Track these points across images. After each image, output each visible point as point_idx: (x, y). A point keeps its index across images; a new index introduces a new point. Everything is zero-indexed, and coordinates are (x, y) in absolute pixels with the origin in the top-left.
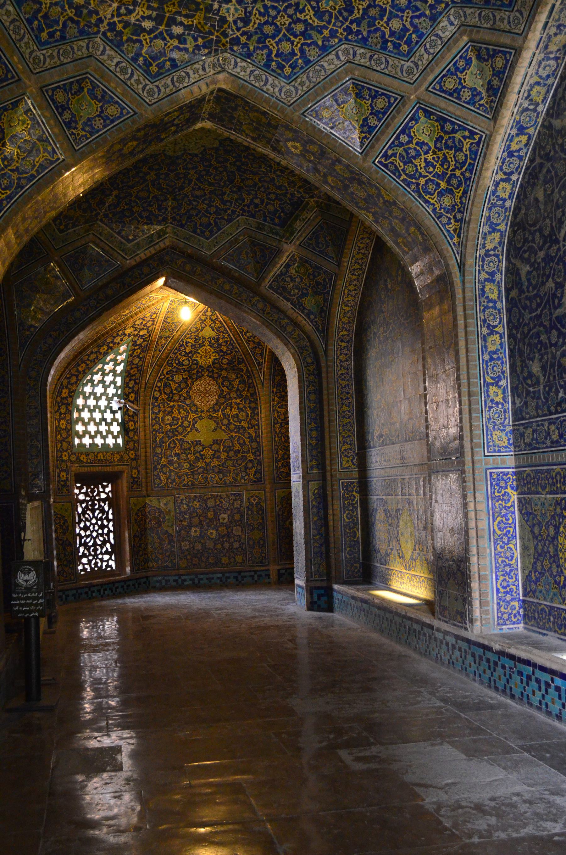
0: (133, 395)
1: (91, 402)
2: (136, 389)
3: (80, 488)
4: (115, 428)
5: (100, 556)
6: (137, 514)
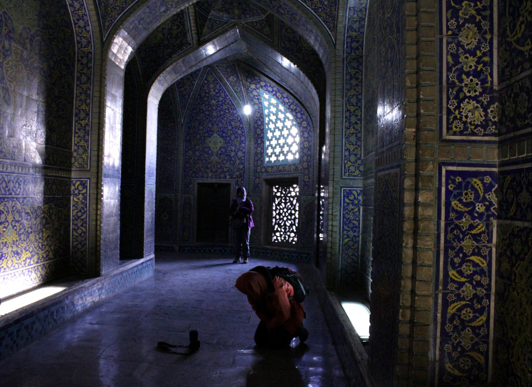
0: (305, 122)
1: (277, 133)
3: (278, 189)
4: (295, 148)
5: (288, 234)
6: (305, 208)
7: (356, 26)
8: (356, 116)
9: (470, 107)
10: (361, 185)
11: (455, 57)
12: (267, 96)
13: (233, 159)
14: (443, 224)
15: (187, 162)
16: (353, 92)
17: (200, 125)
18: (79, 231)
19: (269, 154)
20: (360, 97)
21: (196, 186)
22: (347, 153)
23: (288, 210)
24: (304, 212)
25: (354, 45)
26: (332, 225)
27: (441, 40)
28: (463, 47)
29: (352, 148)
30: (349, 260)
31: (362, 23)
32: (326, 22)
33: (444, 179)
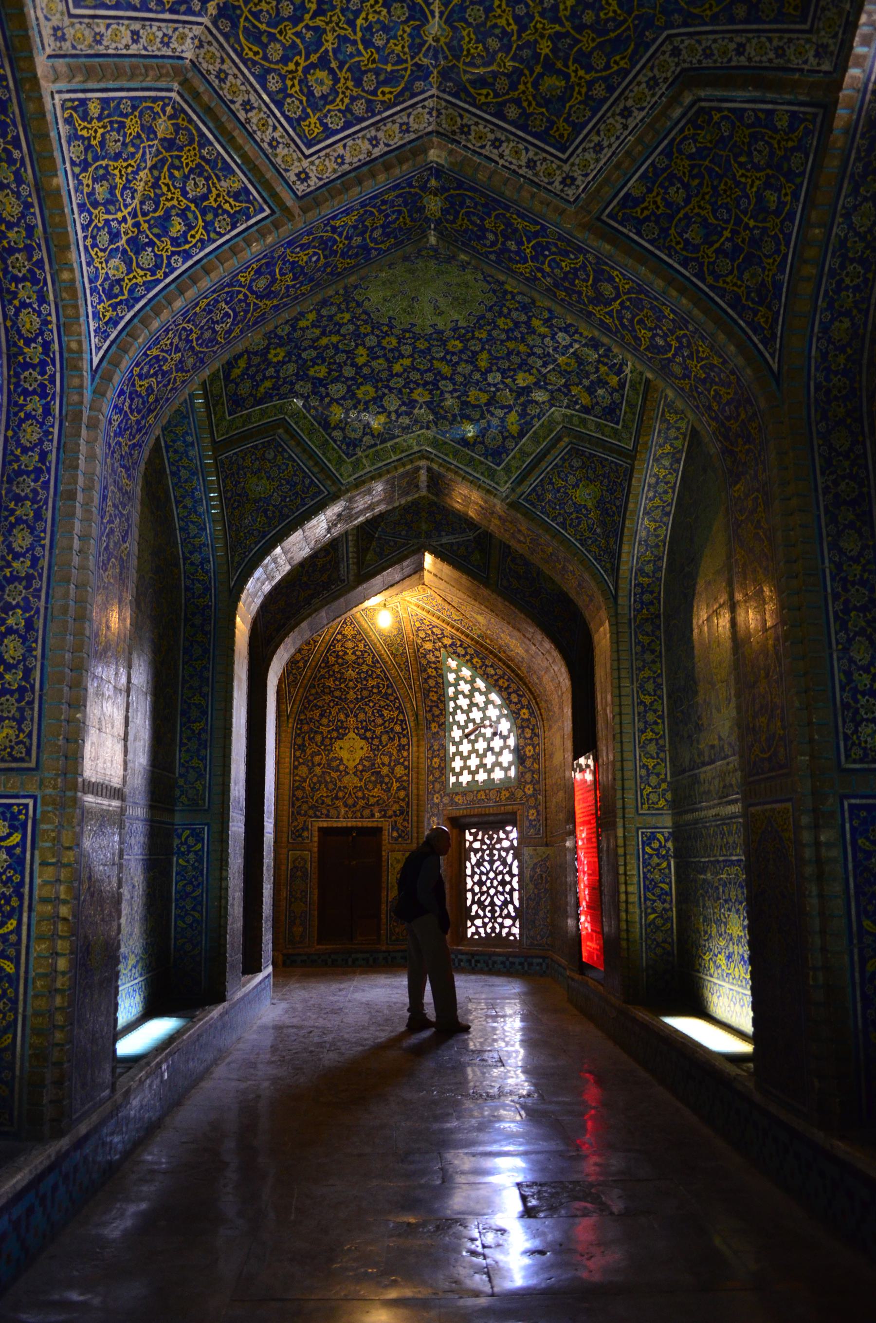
2: (524, 701)
3: (475, 835)
4: (507, 758)
5: (500, 920)
7: (649, 568)
8: (655, 711)
9: (869, 731)
10: (669, 824)
11: (848, 674)
12: (453, 664)
13: (387, 780)
14: (850, 866)
15: (298, 788)
16: (647, 673)
17: (322, 715)
18: (189, 920)
19: (457, 770)
20: (659, 680)
21: (316, 834)
22: (644, 772)
23: (497, 874)
24: (531, 877)
25: (646, 597)
26: (626, 893)
27: (831, 655)
28: (855, 663)
29: (651, 763)
30: (659, 951)
31: (659, 563)
32: (600, 561)
33: (847, 815)
